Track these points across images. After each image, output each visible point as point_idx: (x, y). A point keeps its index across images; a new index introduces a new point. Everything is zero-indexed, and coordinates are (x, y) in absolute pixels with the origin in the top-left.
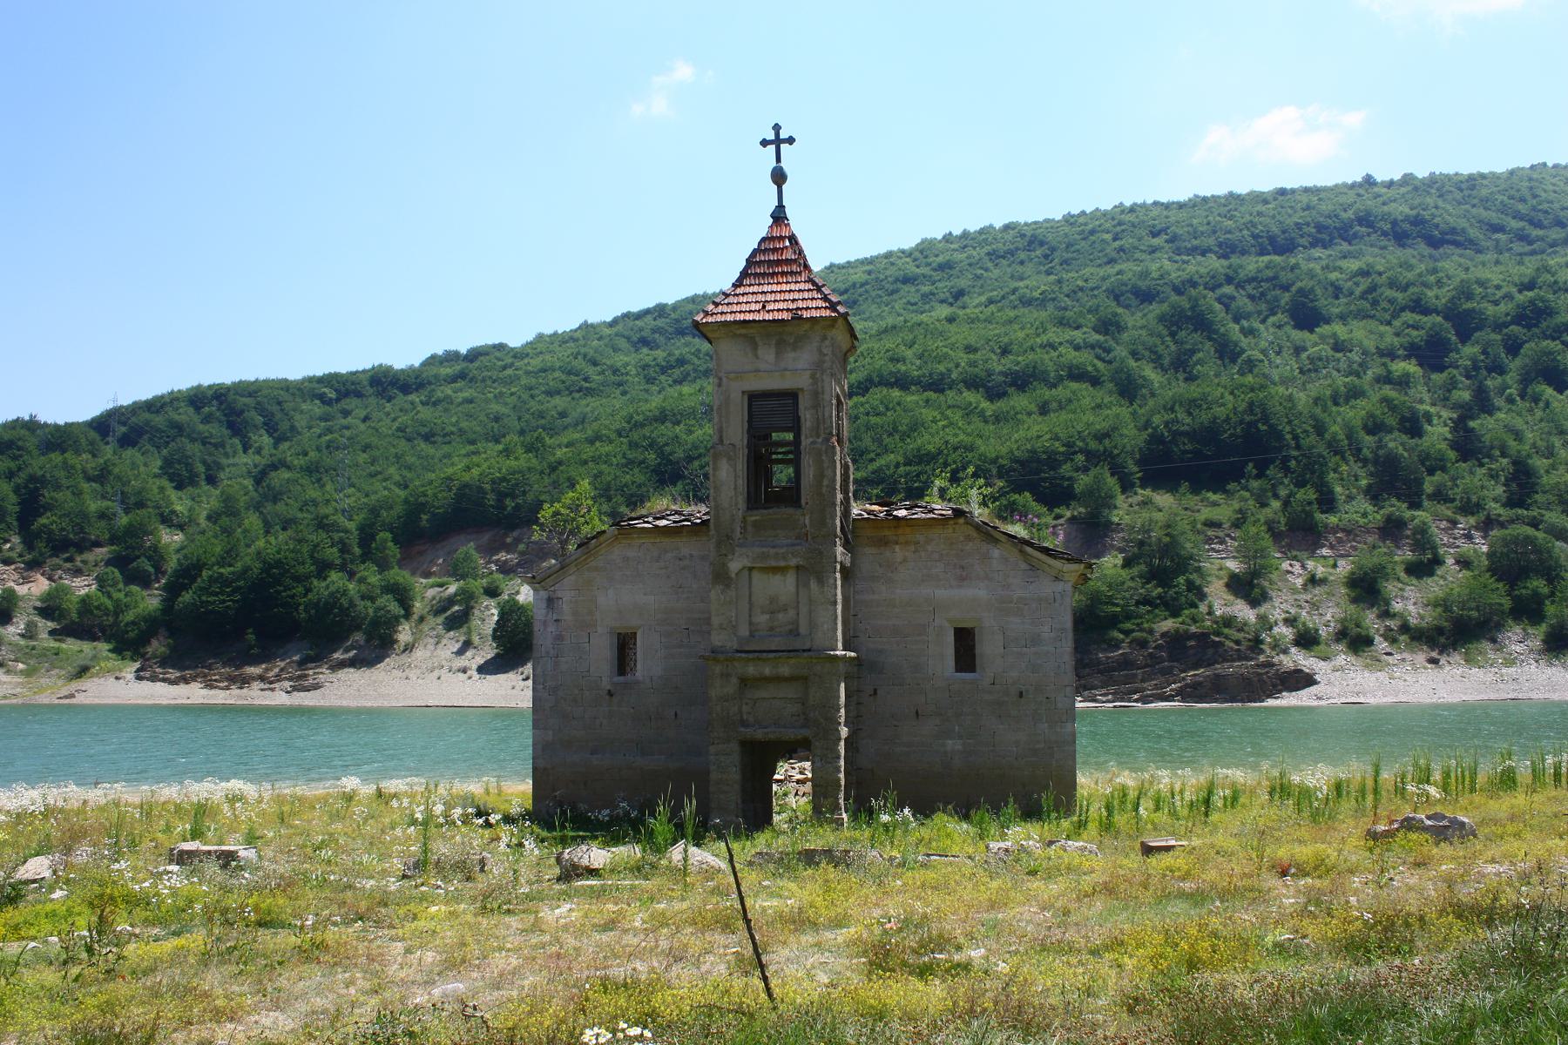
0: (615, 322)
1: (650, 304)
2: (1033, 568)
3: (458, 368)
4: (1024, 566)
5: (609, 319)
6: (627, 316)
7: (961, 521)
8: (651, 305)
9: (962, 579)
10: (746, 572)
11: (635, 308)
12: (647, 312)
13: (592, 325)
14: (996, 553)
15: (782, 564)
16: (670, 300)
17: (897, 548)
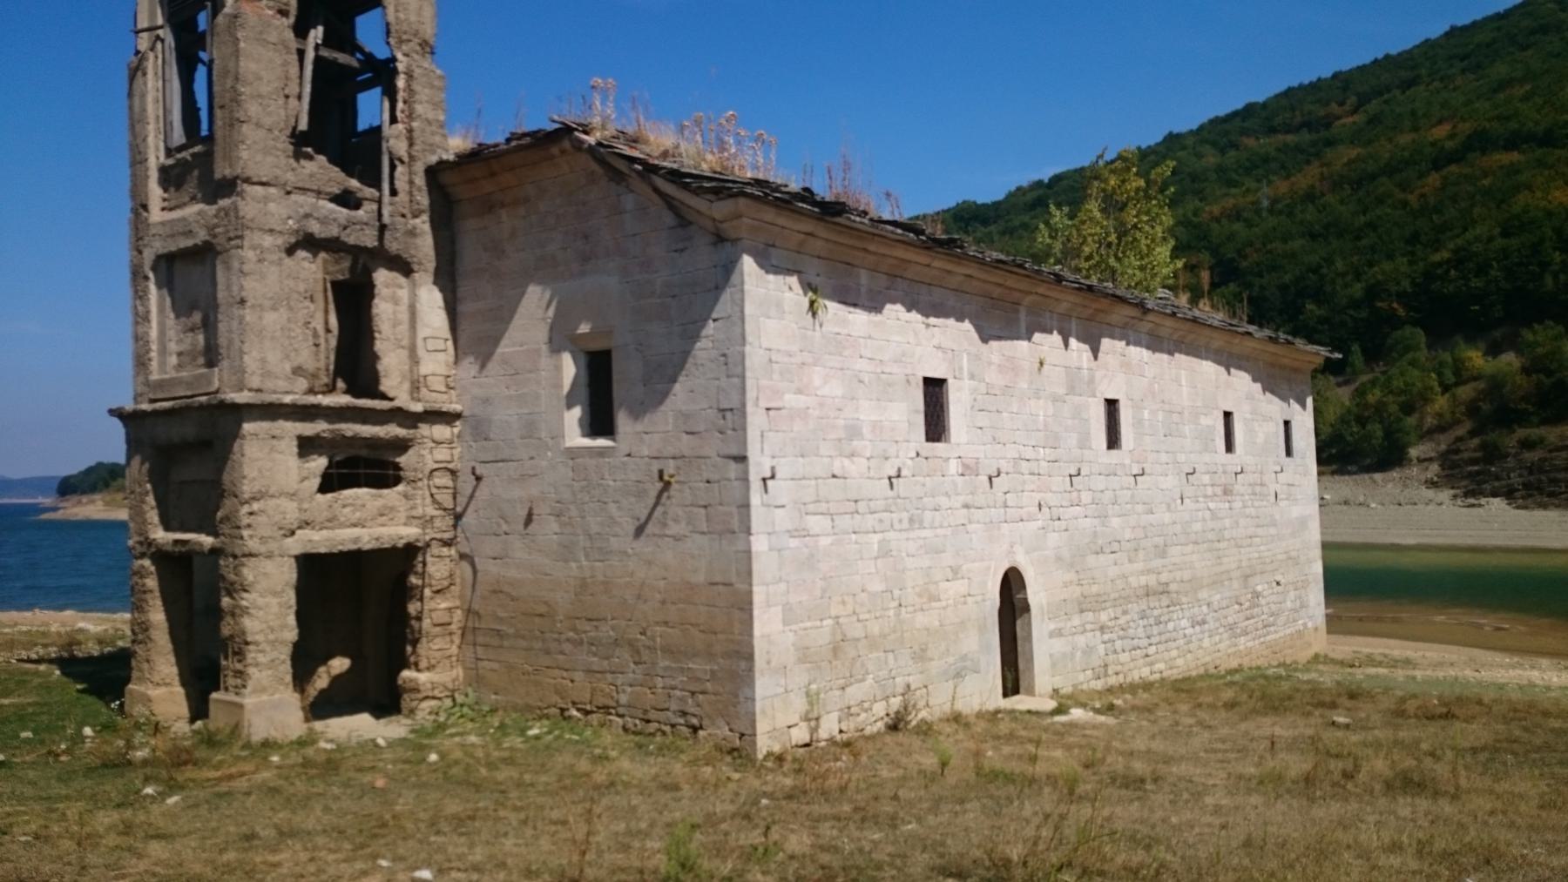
0: (1201, 128)
1: (1239, 105)
2: (683, 220)
3: (1034, 194)
4: (669, 219)
5: (1195, 127)
6: (1215, 122)
7: (566, 144)
8: (1239, 106)
9: (585, 259)
10: (163, 265)
11: (1222, 111)
12: (1235, 114)
13: (1178, 136)
14: (629, 201)
15: (189, 243)
16: (1260, 98)
17: (504, 214)
